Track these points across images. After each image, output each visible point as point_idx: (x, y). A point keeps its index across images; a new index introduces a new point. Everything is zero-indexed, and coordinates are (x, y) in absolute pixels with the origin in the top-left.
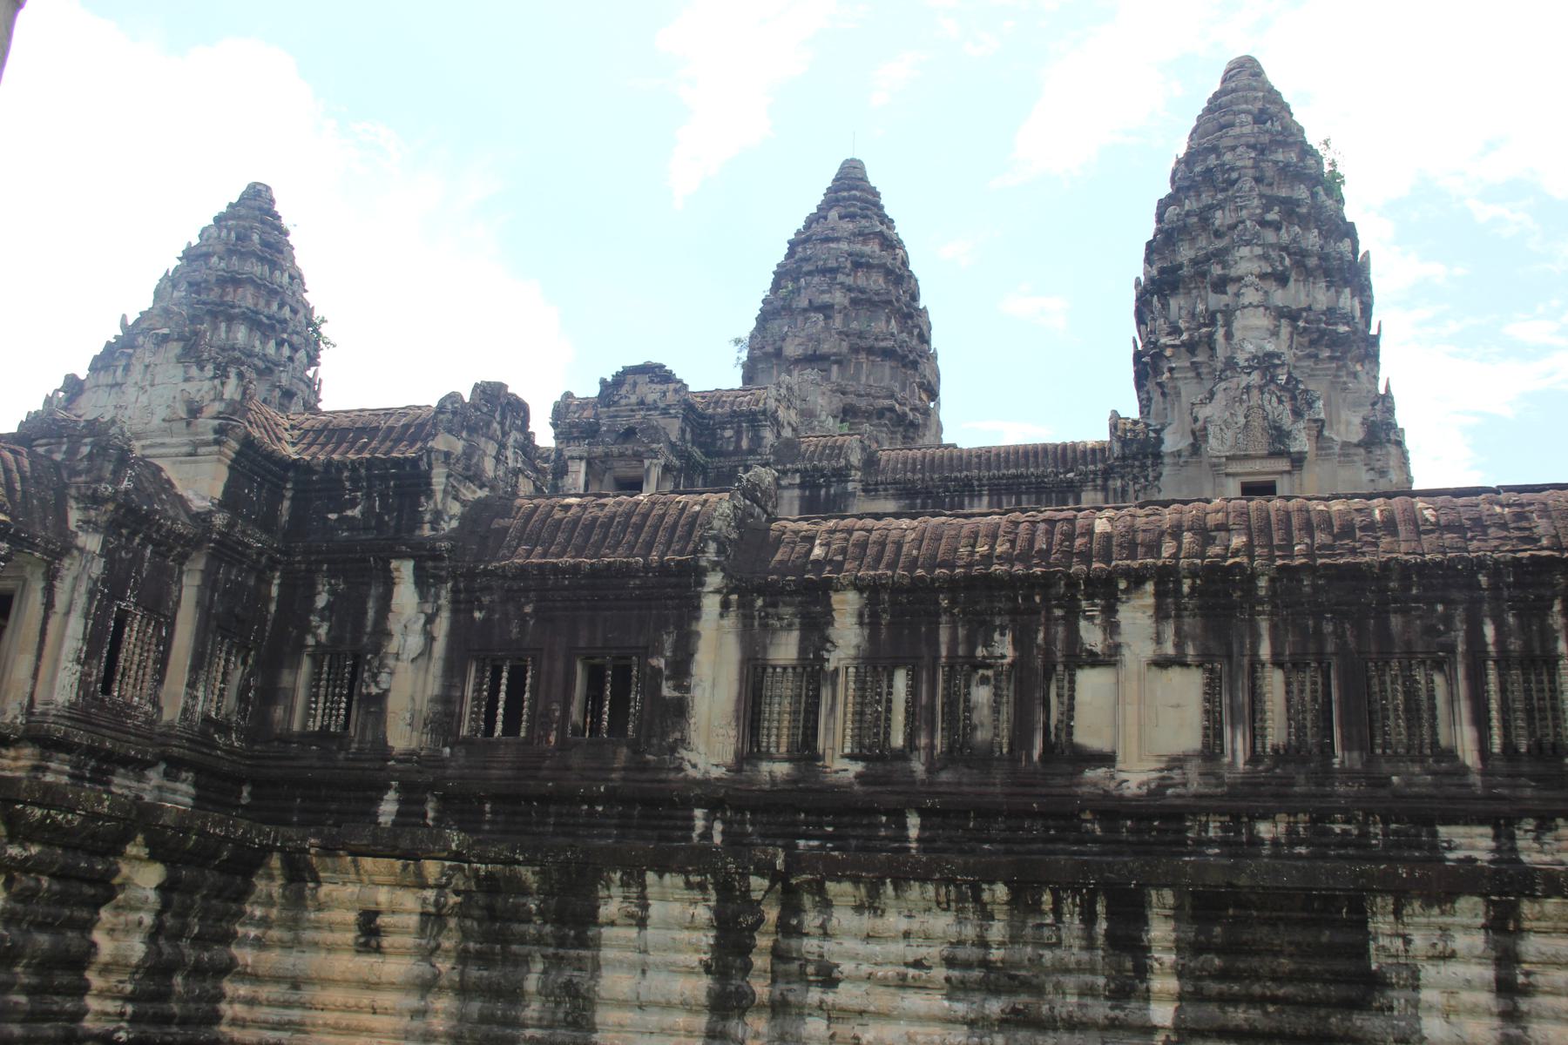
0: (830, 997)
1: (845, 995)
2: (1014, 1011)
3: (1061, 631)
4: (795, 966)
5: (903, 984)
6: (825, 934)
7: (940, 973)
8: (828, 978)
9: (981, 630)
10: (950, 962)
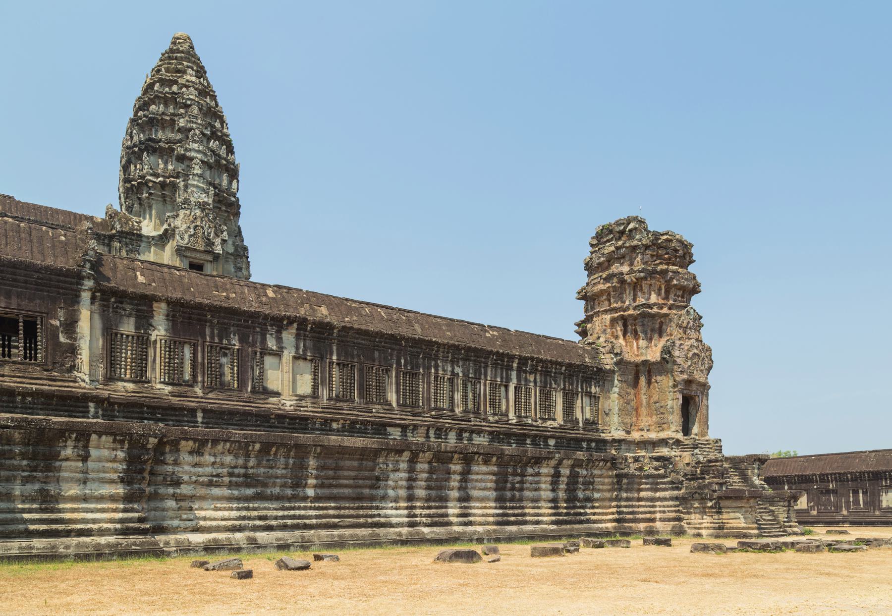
0: (178, 491)
1: (185, 489)
2: (258, 494)
3: (259, 338)
4: (160, 478)
5: (210, 484)
6: (176, 463)
7: (227, 479)
8: (177, 483)
9: (224, 333)
10: (231, 475)
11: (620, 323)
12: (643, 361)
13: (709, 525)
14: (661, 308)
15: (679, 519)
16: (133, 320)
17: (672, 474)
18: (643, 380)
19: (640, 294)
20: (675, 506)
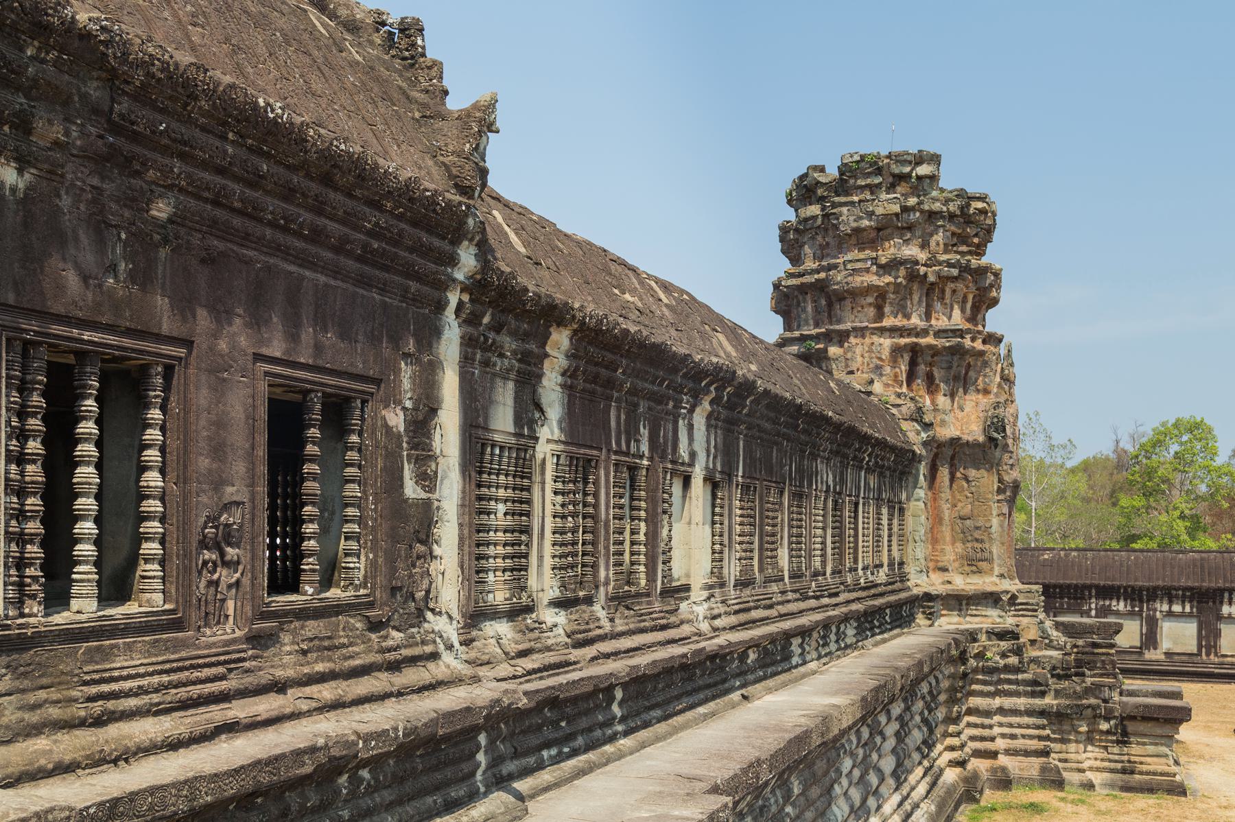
11: (907, 357)
12: (952, 439)
13: (1098, 764)
14: (973, 340)
15: (1045, 753)
16: (511, 385)
17: (1032, 665)
18: (944, 473)
19: (938, 306)
20: (1038, 727)
